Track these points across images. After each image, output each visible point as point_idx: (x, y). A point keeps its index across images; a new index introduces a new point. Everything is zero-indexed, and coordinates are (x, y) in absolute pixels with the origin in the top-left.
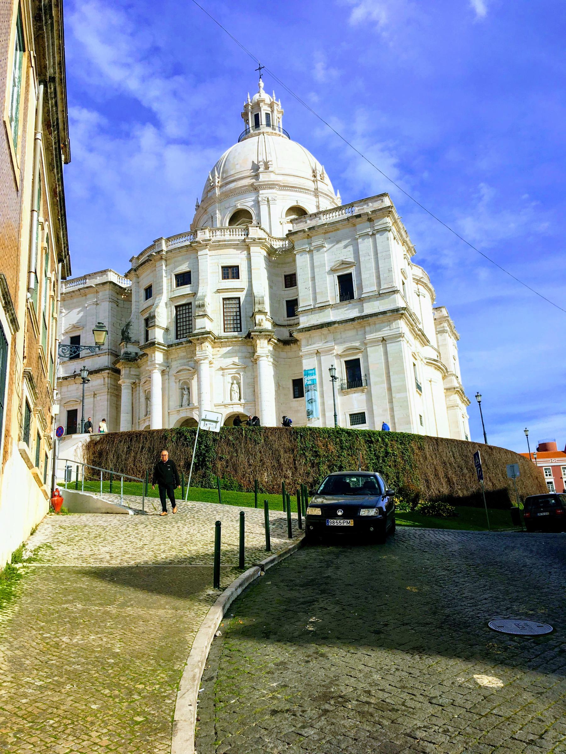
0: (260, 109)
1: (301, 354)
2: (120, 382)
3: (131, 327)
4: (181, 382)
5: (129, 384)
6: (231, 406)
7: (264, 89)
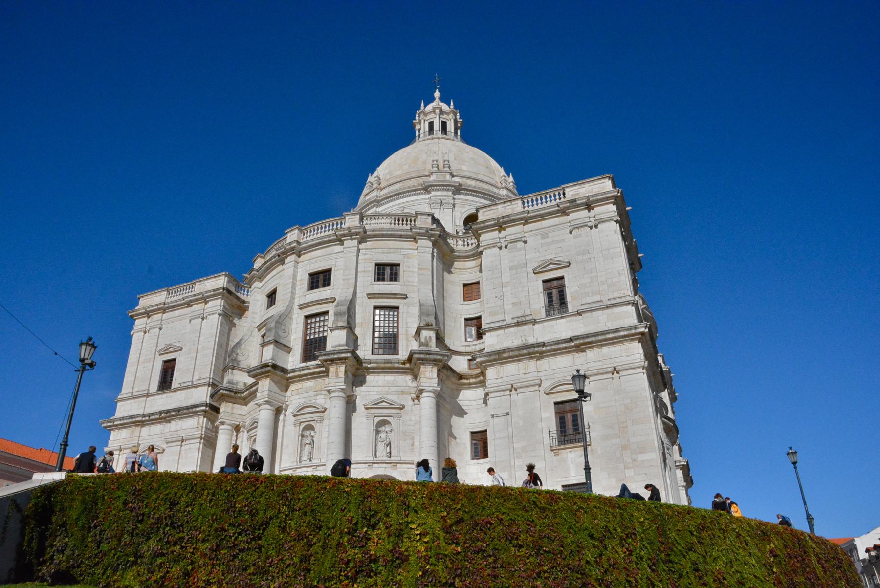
2: (217, 423)
4: (303, 425)
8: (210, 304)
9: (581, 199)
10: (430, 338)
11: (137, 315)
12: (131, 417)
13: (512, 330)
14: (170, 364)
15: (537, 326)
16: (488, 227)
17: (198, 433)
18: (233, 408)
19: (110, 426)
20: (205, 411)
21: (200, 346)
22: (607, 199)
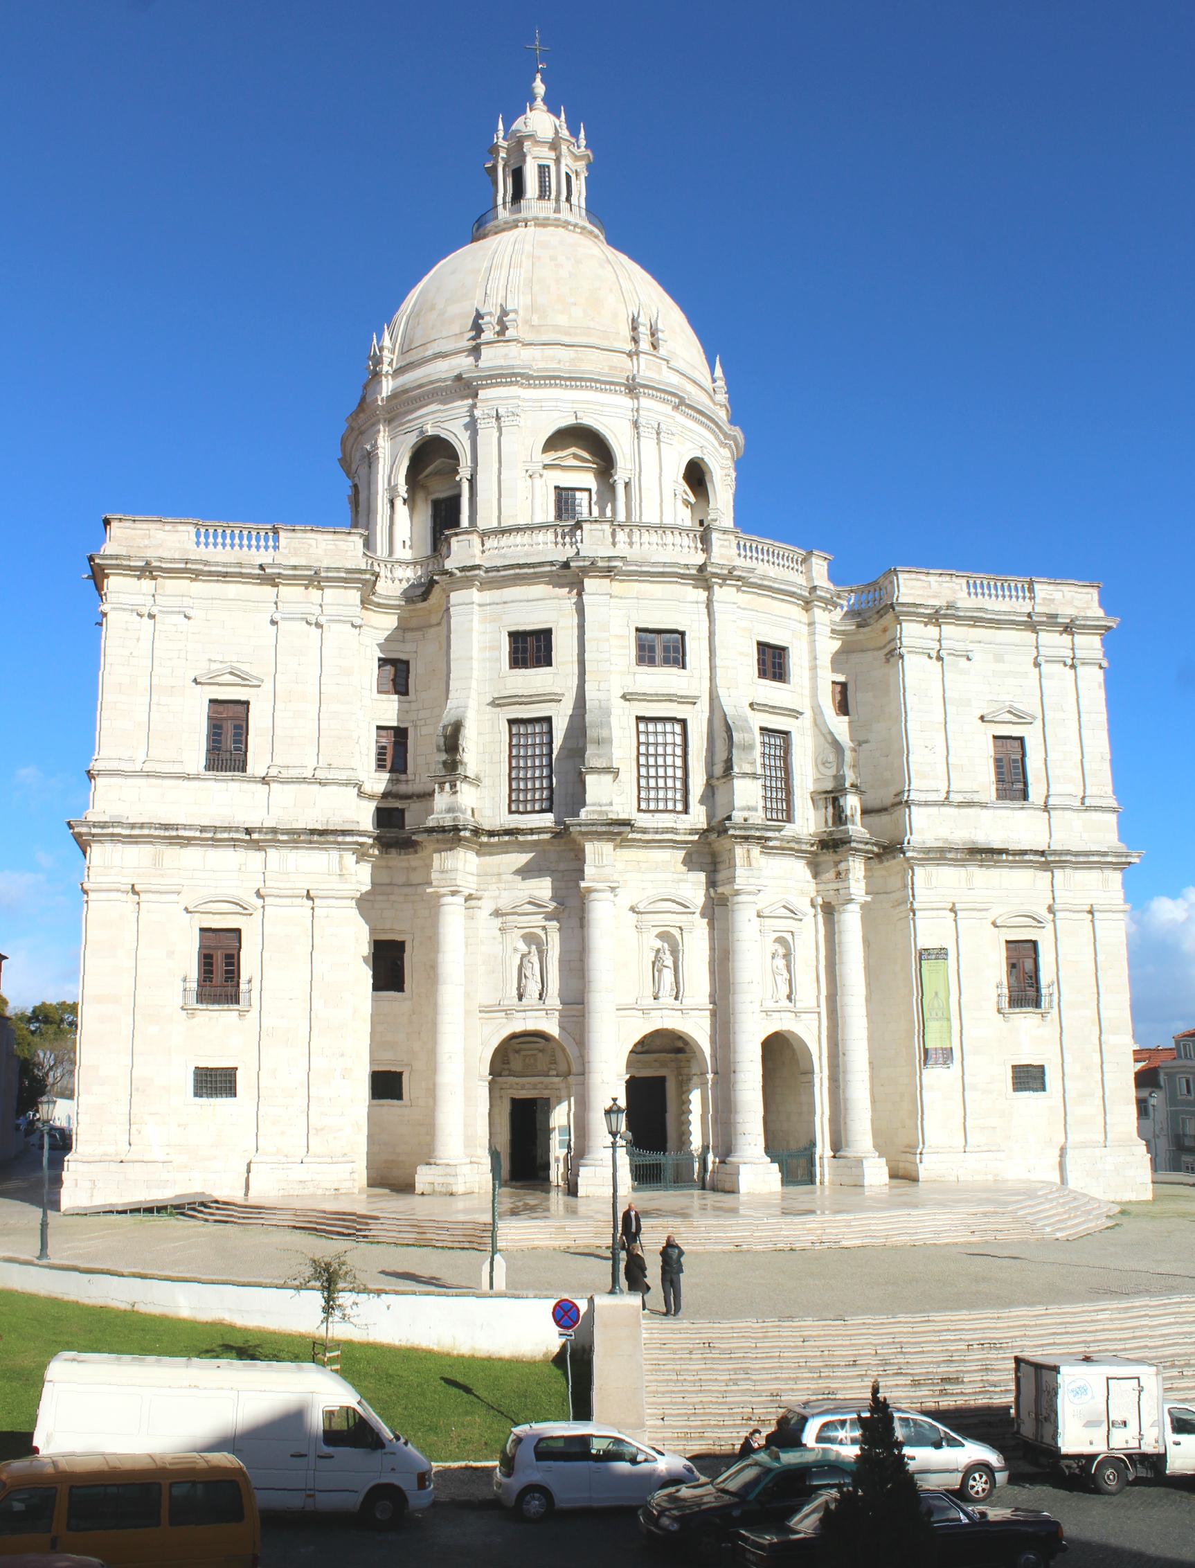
0: (558, 161)
7: (545, 100)
9: (1065, 616)
11: (118, 567)
12: (166, 827)
15: (985, 811)
16: (918, 615)
19: (94, 835)
20: (361, 844)
22: (1097, 627)
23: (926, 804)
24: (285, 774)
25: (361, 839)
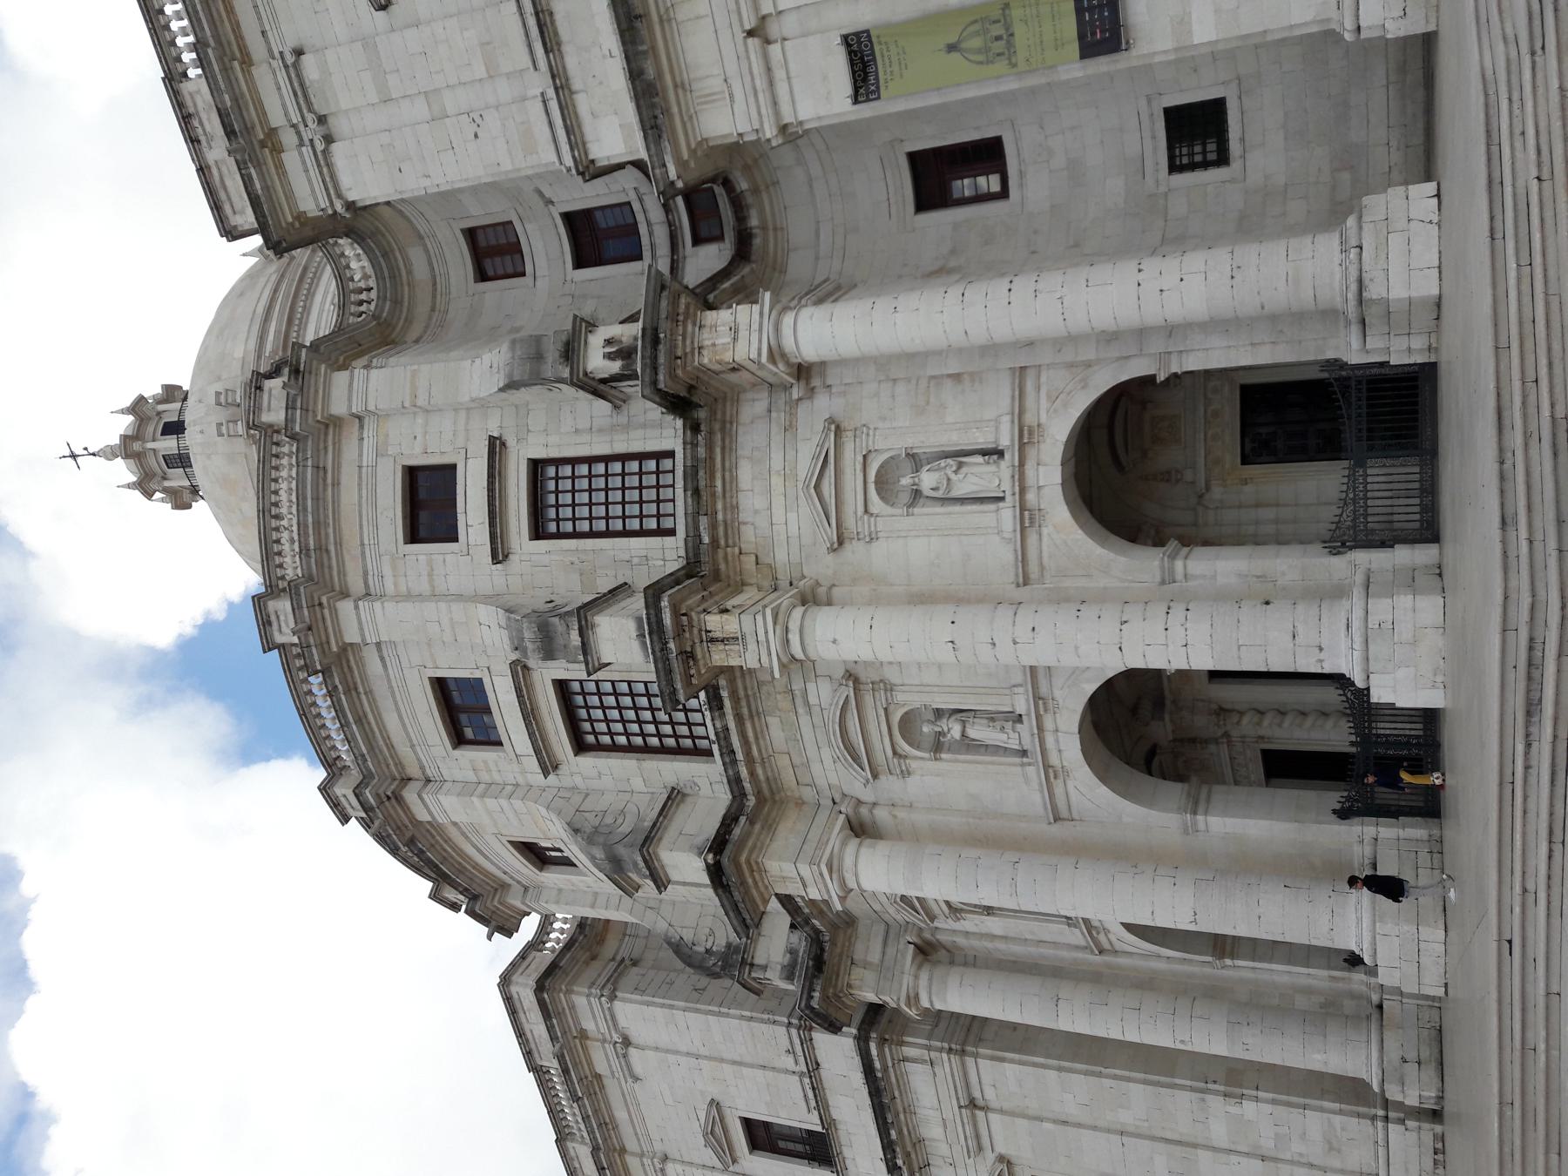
1: (770, 132)
2: (912, 1013)
3: (688, 936)
4: (904, 746)
5: (924, 976)
6: (1031, 497)
8: (588, 1025)
10: (609, 342)
13: (572, 62)
14: (761, 1133)
17: (947, 1064)
18: (866, 965)
20: (882, 1041)
21: (703, 1051)
23: (573, 129)
24: (813, 1103)
25: (874, 1052)
